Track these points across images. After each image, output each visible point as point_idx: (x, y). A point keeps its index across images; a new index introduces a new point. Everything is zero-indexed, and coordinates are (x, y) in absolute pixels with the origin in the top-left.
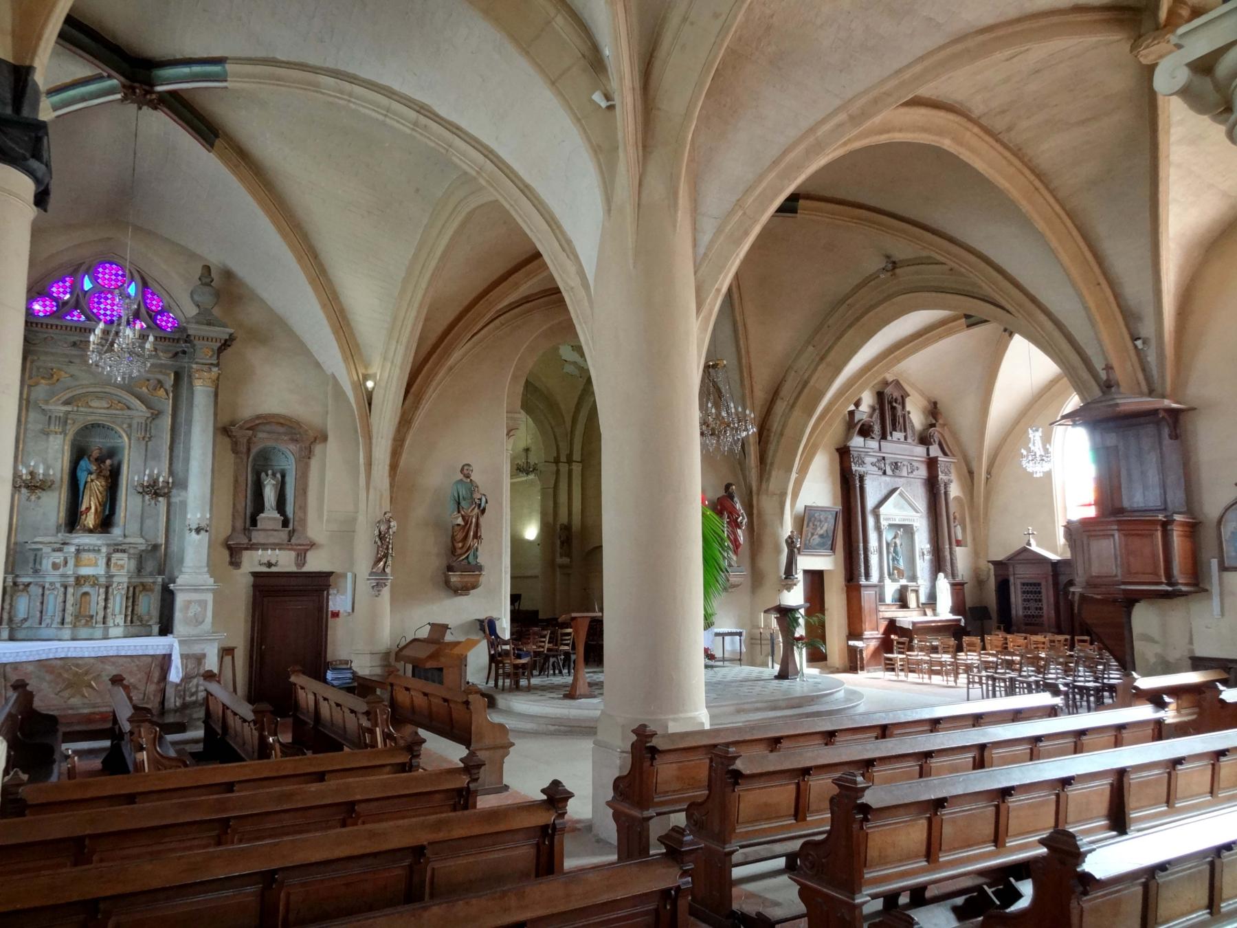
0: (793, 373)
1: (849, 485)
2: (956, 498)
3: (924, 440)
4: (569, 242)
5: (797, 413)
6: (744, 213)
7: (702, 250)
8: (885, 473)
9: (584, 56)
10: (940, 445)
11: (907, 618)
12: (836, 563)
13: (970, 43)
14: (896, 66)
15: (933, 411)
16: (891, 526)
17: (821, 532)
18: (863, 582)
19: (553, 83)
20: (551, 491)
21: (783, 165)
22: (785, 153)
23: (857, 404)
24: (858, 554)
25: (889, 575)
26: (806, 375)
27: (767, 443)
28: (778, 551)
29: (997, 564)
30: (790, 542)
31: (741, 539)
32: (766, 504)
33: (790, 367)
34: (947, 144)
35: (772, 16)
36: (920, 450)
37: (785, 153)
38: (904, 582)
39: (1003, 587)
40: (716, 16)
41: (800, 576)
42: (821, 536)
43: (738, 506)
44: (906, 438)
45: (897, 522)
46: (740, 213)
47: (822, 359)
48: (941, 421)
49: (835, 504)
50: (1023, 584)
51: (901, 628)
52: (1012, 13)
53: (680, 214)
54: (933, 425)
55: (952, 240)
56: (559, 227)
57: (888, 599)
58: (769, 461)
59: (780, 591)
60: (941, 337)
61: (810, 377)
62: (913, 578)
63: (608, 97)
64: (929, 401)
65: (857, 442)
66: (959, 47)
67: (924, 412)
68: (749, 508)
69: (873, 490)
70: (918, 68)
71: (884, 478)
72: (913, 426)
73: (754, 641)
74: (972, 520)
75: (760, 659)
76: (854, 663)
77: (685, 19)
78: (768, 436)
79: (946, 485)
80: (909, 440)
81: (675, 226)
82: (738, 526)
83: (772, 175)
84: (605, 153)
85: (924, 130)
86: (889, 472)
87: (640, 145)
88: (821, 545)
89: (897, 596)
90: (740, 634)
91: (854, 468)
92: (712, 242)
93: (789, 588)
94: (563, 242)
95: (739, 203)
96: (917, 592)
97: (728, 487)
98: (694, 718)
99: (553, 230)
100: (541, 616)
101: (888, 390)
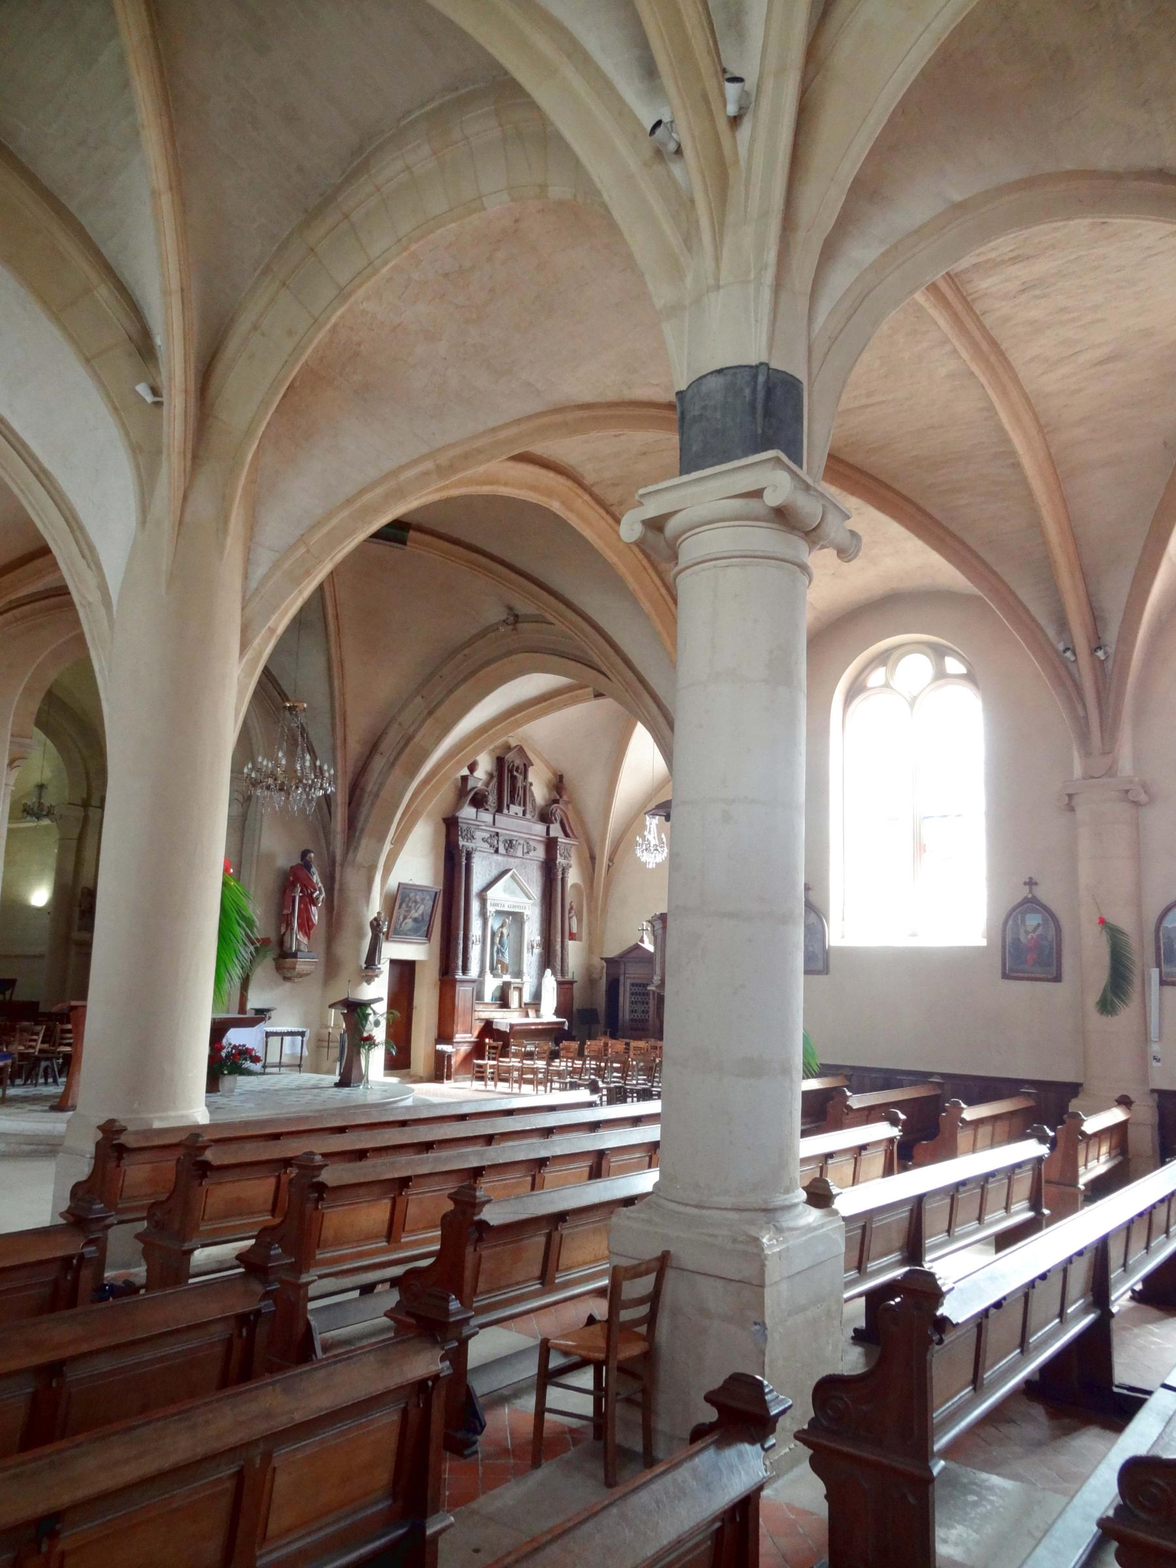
0: (396, 726)
1: (454, 863)
2: (574, 886)
3: (545, 817)
4: (91, 548)
5: (397, 772)
6: (308, 551)
7: (253, 585)
8: (497, 851)
9: (130, 339)
11: (505, 1019)
12: (430, 953)
13: (570, 417)
14: (491, 424)
15: (558, 785)
16: (498, 913)
17: (416, 915)
18: (459, 976)
19: (88, 360)
20: (74, 843)
21: (358, 504)
22: (361, 492)
23: (472, 768)
24: (457, 944)
25: (492, 969)
26: (412, 729)
27: (359, 804)
28: (360, 936)
29: (609, 961)
30: (376, 925)
31: (316, 919)
32: (352, 878)
33: (393, 719)
34: (556, 506)
35: (359, 344)
36: (540, 828)
37: (361, 492)
38: (507, 978)
39: (613, 986)
40: (290, 333)
41: (384, 967)
42: (415, 920)
43: (316, 878)
44: (524, 813)
45: (506, 909)
46: (303, 550)
47: (430, 713)
48: (565, 798)
49: (435, 883)
50: (633, 985)
51: (498, 1031)
52: (611, 396)
53: (229, 541)
54: (556, 801)
55: (568, 604)
56: (81, 528)
57: (488, 997)
58: (360, 825)
59: (360, 984)
60: (566, 705)
61: (416, 731)
62: (519, 974)
63: (155, 391)
64: (555, 774)
65: (468, 812)
66: (558, 418)
67: (548, 786)
68: (330, 881)
69: (481, 871)
70: (512, 431)
71: (496, 857)
72: (534, 800)
73: (321, 1042)
74: (590, 911)
75: (326, 1065)
76: (440, 1071)
77: (255, 328)
78: (361, 796)
80: (528, 816)
81: (222, 553)
82: (314, 902)
83: (344, 514)
84: (146, 455)
85: (534, 488)
86: (502, 850)
87: (189, 456)
88: (415, 931)
89: (498, 994)
90: (302, 1034)
91: (461, 843)
92: (266, 577)
93: (369, 980)
94: (84, 546)
95: (302, 540)
96: (520, 990)
97: (305, 854)
98: (183, 1116)
99: (72, 531)
100: (42, 1009)
101: (509, 757)
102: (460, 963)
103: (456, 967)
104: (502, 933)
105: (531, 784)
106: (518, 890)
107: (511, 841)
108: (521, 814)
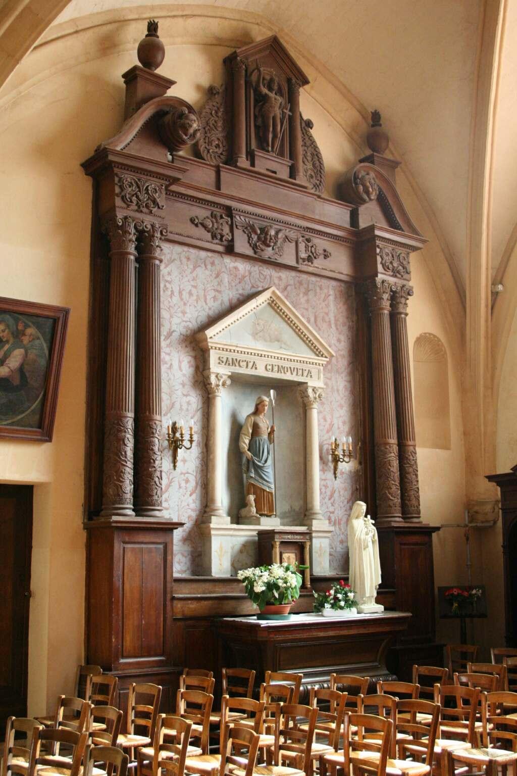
3: (347, 191)
10: (382, 201)
16: (240, 382)
36: (336, 214)
38: (269, 524)
44: (293, 172)
45: (261, 372)
64: (362, 111)
67: (351, 137)
71: (228, 261)
72: (316, 155)
79: (394, 298)
80: (301, 179)
86: (242, 245)
102: (128, 487)
103: (119, 497)
104: (256, 427)
105: (309, 124)
106: (288, 333)
107: (264, 231)
108: (284, 174)
